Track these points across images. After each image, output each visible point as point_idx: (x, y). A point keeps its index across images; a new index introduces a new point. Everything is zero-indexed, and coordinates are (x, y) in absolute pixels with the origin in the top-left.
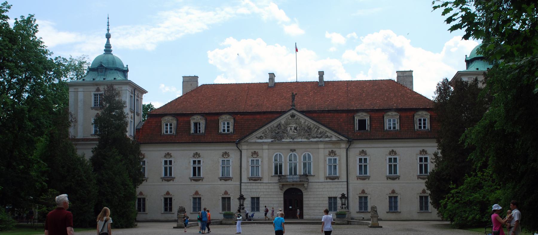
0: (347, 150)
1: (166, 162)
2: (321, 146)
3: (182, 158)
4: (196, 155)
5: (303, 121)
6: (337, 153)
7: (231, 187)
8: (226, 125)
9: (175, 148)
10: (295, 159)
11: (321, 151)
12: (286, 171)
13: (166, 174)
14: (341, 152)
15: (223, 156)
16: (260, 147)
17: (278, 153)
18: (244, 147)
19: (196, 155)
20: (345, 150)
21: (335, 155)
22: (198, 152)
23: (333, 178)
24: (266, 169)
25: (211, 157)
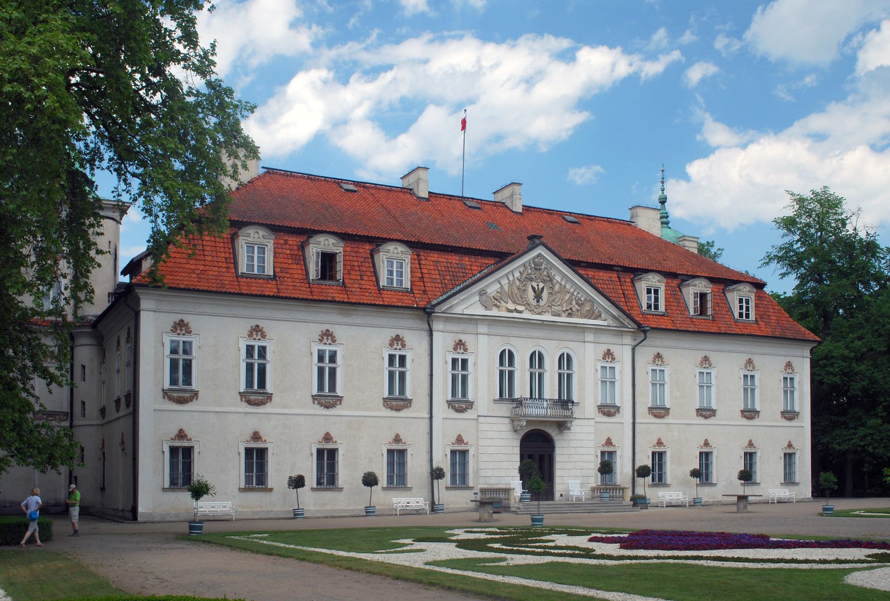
0: (633, 350)
1: (250, 350)
2: (589, 337)
3: (293, 340)
4: (327, 335)
5: (558, 278)
6: (616, 355)
7: (410, 426)
8: (394, 265)
9: (279, 314)
10: (511, 363)
11: (590, 347)
12: (521, 389)
13: (249, 383)
14: (623, 352)
15: (391, 345)
16: (470, 328)
17: (507, 348)
18: (437, 326)
19: (327, 335)
20: (629, 349)
21: (613, 359)
22: (332, 328)
23: (608, 410)
24: (483, 383)
25: (363, 344)
